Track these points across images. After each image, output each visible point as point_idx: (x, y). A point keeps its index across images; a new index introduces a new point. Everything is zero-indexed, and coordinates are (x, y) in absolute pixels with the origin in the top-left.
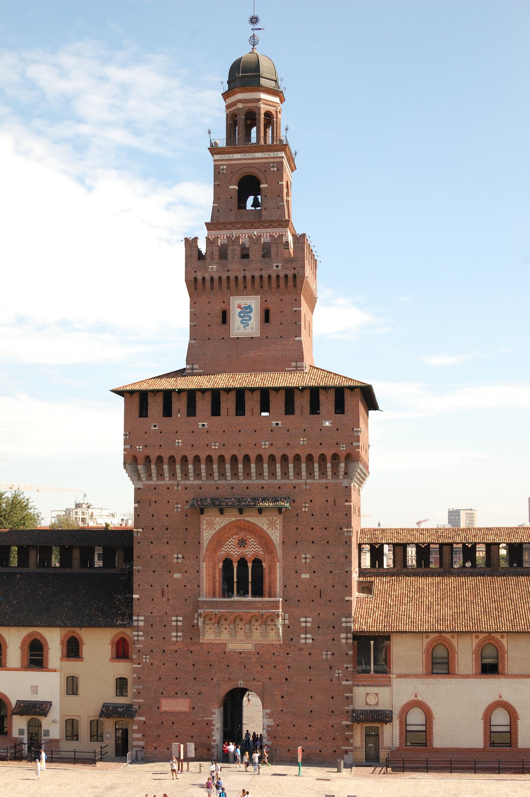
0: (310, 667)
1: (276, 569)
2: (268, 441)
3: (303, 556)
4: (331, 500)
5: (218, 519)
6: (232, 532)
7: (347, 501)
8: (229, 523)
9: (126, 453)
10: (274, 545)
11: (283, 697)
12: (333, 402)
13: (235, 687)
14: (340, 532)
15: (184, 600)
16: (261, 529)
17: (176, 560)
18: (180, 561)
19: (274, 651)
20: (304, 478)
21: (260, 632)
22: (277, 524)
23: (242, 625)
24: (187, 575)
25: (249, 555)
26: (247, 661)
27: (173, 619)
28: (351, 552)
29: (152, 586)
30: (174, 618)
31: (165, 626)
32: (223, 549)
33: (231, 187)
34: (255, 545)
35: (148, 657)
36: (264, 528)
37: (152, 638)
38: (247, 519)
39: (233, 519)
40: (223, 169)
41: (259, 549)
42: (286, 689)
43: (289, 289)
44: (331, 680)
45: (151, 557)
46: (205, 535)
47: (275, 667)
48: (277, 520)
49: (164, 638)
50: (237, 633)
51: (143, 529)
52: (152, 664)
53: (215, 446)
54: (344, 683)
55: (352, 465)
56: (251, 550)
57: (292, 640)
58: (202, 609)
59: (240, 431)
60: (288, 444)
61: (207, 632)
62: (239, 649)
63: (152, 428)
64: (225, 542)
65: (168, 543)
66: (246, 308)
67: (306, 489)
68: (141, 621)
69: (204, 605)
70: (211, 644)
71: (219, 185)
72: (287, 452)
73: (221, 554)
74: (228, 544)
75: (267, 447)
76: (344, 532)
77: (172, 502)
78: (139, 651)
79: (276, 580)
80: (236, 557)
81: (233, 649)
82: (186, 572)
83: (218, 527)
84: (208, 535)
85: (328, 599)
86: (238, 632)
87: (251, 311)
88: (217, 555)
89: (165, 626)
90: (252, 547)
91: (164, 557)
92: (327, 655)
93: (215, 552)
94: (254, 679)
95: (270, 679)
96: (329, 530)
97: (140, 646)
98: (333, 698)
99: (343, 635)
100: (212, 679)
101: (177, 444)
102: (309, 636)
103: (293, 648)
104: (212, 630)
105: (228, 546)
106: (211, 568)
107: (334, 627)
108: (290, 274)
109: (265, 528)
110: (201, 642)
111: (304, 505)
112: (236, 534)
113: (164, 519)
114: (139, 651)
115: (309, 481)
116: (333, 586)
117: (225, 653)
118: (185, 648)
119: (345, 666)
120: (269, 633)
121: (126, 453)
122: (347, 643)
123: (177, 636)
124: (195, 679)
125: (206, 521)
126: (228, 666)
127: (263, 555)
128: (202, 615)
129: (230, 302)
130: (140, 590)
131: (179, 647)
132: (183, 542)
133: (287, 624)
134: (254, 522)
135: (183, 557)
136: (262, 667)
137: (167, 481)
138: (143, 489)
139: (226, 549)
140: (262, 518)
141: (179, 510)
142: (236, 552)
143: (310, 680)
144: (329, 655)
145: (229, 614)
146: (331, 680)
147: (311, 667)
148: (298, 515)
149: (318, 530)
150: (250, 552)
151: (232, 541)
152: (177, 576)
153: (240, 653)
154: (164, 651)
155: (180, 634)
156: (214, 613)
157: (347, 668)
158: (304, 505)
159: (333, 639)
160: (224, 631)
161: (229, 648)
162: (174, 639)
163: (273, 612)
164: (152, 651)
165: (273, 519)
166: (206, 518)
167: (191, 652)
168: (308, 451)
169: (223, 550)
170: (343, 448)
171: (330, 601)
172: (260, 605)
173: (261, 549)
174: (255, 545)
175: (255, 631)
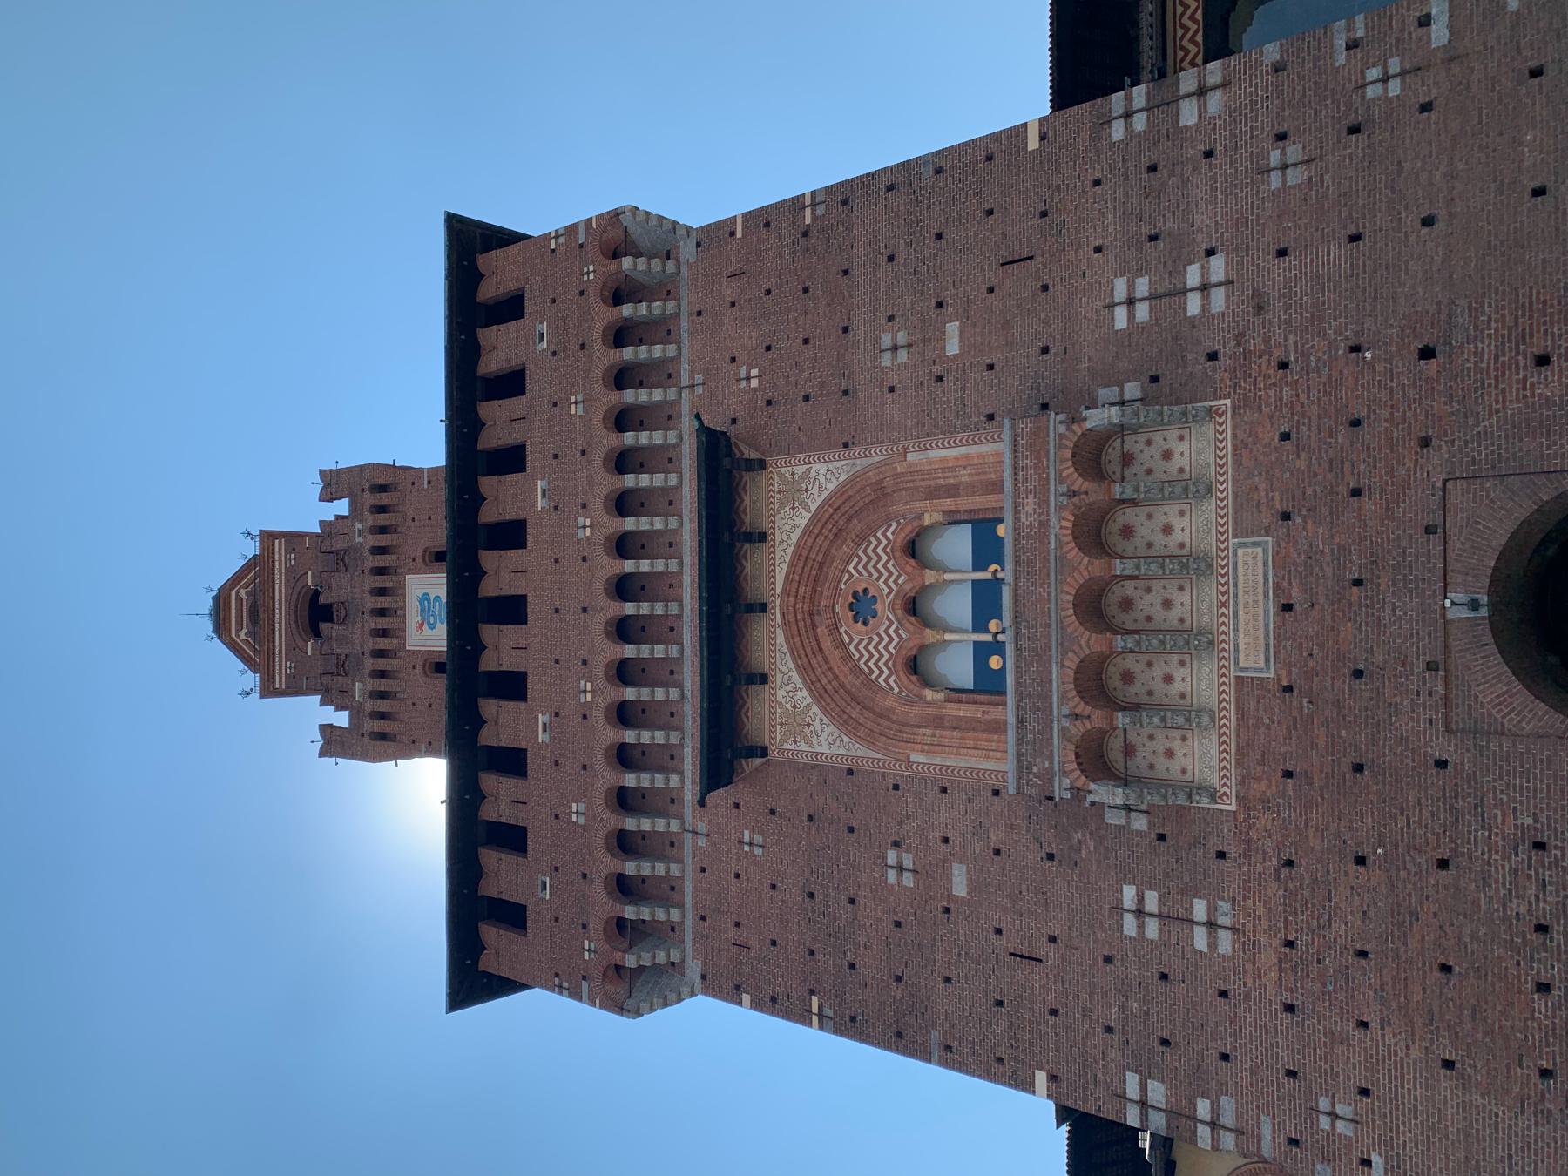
0: (1355, 238)
1: (930, 462)
2: (576, 518)
3: (886, 360)
4: (728, 290)
5: (781, 693)
6: (827, 643)
7: (732, 234)
8: (792, 653)
9: (598, 1000)
10: (852, 480)
11: (1543, 360)
12: (503, 327)
13: (1488, 637)
14: (814, 233)
15: (1052, 867)
16: (807, 531)
17: (906, 874)
18: (908, 862)
19: (1269, 435)
20: (672, 394)
21: (1182, 513)
22: (793, 474)
23: (1148, 598)
24: (955, 838)
25: (900, 582)
26: (1329, 571)
27: (1134, 934)
28: (873, 175)
29: (1000, 1003)
30: (1129, 925)
31: (1164, 977)
32: (881, 680)
33: (309, 654)
34: (870, 559)
35: (1324, 1104)
36: (804, 522)
37: (1225, 1057)
38: (779, 590)
39: (780, 638)
40: (290, 668)
41: (880, 542)
42: (1488, 347)
43: (395, 501)
44: (1426, 108)
45: (899, 979)
46: (825, 749)
47: (1356, 423)
48: (781, 475)
49: (1223, 994)
50: (1187, 625)
51: (812, 992)
52: (1365, 1092)
53: (585, 691)
54: (1439, 33)
55: (636, 232)
56: (883, 570)
57: (1213, 356)
58: (1051, 781)
59: (557, 611)
60: (583, 453)
61: (1184, 771)
62: (1266, 611)
63: (548, 897)
64: (862, 671)
65: (852, 901)
66: (423, 609)
67: (704, 384)
68: (1144, 1089)
69: (1035, 769)
70: (1241, 753)
71: (307, 679)
72: (598, 455)
73: (896, 690)
74: (866, 663)
75: (588, 523)
76: (815, 218)
77: (738, 860)
78: (1293, 1142)
79: (967, 457)
80: (907, 631)
81: (1267, 646)
82: (946, 840)
83: (804, 697)
84: (825, 735)
85: (1037, 222)
86: (1182, 620)
87: (426, 597)
88: (895, 705)
89: (1164, 977)
90: (875, 567)
91: (898, 924)
92: (1284, 167)
93: (884, 715)
94: (1429, 530)
95: (1425, 442)
96: (810, 277)
97: (1266, 1131)
98: (1536, 73)
99: (1188, 114)
100: (1441, 764)
101: (582, 820)
102: (1193, 276)
103: (1254, 342)
104: (1177, 745)
105: (871, 664)
106: (938, 732)
107: (1153, 169)
108: (369, 499)
109: (802, 519)
110: (1233, 808)
111: (744, 383)
112: (835, 628)
113: (783, 901)
114: (1293, 1142)
115: (685, 381)
116: (990, 212)
117: (1288, 689)
118: (1269, 892)
119: (1341, 58)
120: (1181, 470)
121: (598, 1000)
122: (1225, 84)
123: (1211, 925)
124: (1443, 864)
125: (784, 741)
126: (1358, 674)
127: (898, 522)
128: (1079, 784)
129: (413, 652)
130: (1017, 1060)
131: (1265, 924)
132: (847, 836)
133: (1143, 390)
134: (788, 559)
135: (896, 844)
136: (1356, 492)
137: (684, 870)
138: (704, 963)
139: (882, 672)
140: (777, 532)
141: (758, 839)
142: (891, 631)
143: (1428, 222)
144: (1284, 153)
145: (1070, 655)
146: (1426, 108)
147: (1352, 230)
148: (769, 403)
149: (810, 316)
150: (891, 574)
151: (856, 647)
152: (960, 885)
153: (1288, 607)
154: (1290, 1008)
155: (1200, 910)
156: (1066, 723)
157: (1352, 45)
158: (744, 383)
159: (1209, 154)
160: (1177, 686)
161: (1262, 664)
162: (1225, 941)
163: (1061, 446)
164: (1292, 1074)
165: (779, 492)
166: (778, 737)
167: (1289, 863)
168: (597, 386)
169: (886, 681)
170: (591, 273)
171: (1044, 214)
172: (1030, 504)
173: (879, 535)
174: (870, 559)
175: (1177, 536)
